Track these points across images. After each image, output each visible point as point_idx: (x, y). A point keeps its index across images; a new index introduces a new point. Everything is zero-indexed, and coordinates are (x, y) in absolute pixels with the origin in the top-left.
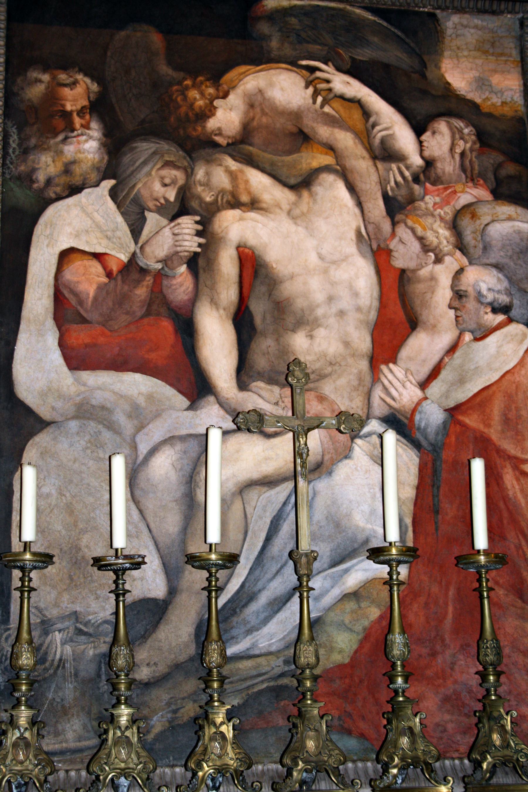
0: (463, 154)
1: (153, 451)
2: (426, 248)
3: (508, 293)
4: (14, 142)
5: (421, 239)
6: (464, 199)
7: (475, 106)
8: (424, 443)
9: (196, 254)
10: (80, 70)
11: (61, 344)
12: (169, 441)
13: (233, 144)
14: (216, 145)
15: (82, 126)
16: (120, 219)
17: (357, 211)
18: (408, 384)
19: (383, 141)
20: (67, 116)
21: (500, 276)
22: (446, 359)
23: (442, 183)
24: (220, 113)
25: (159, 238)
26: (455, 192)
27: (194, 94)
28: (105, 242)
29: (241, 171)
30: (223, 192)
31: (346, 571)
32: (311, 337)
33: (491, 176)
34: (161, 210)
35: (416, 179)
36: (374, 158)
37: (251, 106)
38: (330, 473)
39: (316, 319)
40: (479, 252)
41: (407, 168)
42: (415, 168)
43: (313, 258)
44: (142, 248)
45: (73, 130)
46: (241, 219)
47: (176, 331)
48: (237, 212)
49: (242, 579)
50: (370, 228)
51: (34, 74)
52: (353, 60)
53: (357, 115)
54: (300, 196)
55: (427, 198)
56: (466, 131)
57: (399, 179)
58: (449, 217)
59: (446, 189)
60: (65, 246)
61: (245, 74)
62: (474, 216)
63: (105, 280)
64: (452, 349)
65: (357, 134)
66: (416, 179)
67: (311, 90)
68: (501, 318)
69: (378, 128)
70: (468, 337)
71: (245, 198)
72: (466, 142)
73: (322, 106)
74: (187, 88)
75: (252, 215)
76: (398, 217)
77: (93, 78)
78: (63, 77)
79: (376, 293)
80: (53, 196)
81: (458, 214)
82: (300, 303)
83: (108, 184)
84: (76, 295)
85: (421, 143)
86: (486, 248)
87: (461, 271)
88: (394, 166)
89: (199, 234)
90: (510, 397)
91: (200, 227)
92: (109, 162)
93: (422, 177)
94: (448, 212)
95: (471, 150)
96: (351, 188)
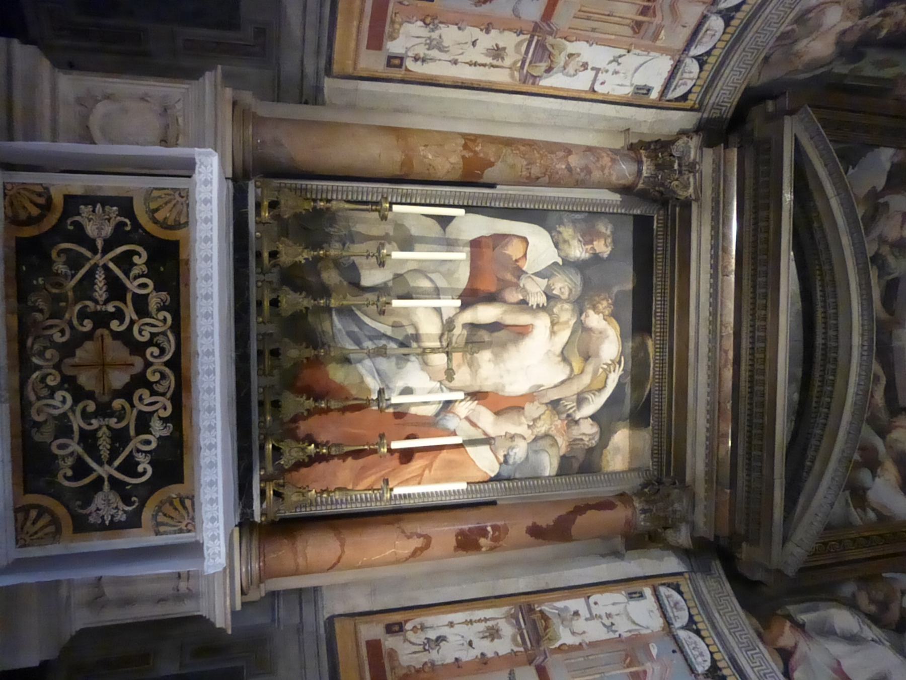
0: (582, 440)
1: (431, 280)
3: (514, 463)
4: (578, 216)
5: (539, 418)
7: (606, 446)
8: (438, 418)
9: (528, 304)
10: (613, 249)
13: (582, 324)
14: (581, 314)
15: (587, 249)
16: (543, 267)
17: (552, 385)
18: (467, 410)
19: (587, 399)
20: (591, 242)
21: (523, 459)
22: (480, 430)
23: (568, 429)
24: (596, 316)
26: (563, 436)
27: (605, 303)
30: (558, 317)
31: (374, 377)
32: (489, 361)
34: (548, 286)
35: (569, 416)
36: (578, 394)
37: (601, 333)
38: (422, 369)
41: (574, 411)
42: (574, 415)
44: (530, 277)
45: (585, 245)
46: (546, 327)
48: (549, 324)
49: (370, 324)
51: (610, 227)
52: (625, 384)
54: (558, 356)
55: (560, 421)
56: (594, 442)
57: (569, 407)
58: (550, 433)
59: (565, 431)
61: (615, 329)
62: (552, 445)
63: (514, 259)
65: (589, 385)
67: (610, 362)
68: (502, 459)
69: (593, 396)
71: (556, 328)
72: (588, 441)
73: (602, 368)
74: (608, 301)
75: (548, 332)
76: (550, 406)
77: (610, 255)
78: (609, 240)
80: (553, 234)
81: (552, 437)
82: (506, 355)
84: (506, 245)
85: (586, 418)
86: (536, 452)
87: (525, 439)
88: (575, 404)
89: (538, 305)
91: (541, 306)
92: (571, 262)
93: (570, 418)
94: (553, 432)
95: (584, 444)
96: (563, 382)
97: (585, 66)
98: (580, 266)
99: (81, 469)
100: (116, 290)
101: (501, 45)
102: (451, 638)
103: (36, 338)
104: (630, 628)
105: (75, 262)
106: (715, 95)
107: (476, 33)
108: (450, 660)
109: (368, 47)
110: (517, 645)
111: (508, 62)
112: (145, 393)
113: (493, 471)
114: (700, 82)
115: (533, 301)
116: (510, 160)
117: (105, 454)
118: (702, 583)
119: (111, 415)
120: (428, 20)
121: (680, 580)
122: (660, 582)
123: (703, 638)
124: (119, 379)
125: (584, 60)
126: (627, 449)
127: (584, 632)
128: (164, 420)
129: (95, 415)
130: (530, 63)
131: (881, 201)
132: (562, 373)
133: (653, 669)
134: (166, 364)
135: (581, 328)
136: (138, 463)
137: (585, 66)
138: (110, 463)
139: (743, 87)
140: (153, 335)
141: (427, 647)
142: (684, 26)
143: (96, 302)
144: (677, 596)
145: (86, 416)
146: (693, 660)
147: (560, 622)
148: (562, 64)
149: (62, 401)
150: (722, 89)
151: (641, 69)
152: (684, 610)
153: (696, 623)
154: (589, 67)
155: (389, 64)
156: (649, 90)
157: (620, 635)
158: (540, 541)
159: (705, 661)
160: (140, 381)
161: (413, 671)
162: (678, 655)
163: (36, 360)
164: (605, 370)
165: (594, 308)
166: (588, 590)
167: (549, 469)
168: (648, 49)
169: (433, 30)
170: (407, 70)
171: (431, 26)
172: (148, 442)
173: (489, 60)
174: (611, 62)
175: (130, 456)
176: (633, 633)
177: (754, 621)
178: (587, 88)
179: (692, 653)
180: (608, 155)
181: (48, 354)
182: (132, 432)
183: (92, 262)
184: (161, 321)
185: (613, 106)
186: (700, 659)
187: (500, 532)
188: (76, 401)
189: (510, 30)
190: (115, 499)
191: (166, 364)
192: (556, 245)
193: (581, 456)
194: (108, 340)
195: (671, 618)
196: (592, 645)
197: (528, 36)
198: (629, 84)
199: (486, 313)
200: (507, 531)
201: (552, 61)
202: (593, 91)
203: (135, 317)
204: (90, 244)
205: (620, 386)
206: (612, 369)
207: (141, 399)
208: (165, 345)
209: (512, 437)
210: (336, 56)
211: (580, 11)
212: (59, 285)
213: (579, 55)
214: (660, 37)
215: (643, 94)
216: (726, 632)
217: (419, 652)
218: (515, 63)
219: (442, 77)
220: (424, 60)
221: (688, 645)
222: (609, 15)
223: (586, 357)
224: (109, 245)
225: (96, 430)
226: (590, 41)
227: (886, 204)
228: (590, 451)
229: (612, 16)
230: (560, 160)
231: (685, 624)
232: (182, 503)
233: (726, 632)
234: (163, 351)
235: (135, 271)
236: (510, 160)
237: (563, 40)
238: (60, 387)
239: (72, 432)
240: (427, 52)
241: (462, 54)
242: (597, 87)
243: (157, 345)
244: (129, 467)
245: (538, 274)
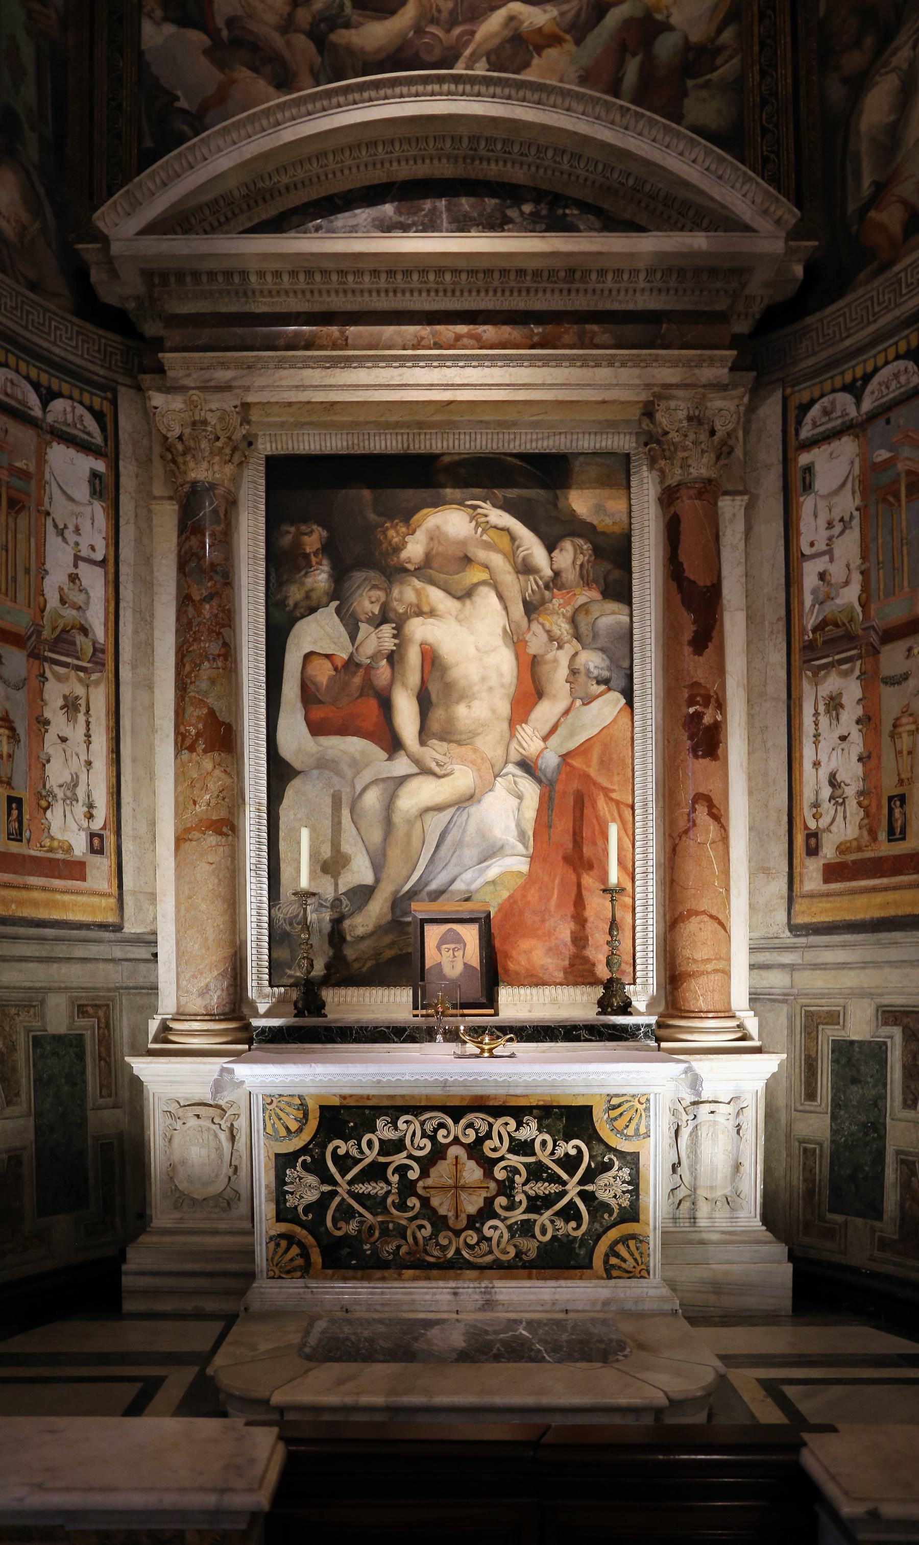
0: (582, 566)
1: (365, 789)
2: (551, 638)
5: (548, 632)
6: (581, 600)
7: (592, 527)
8: (544, 779)
9: (393, 651)
11: (307, 719)
12: (375, 782)
14: (406, 570)
16: (342, 629)
17: (504, 613)
19: (524, 559)
20: (306, 556)
24: (410, 547)
25: (368, 641)
27: (391, 533)
28: (333, 646)
29: (424, 589)
30: (411, 605)
31: (488, 867)
33: (602, 582)
34: (369, 621)
35: (547, 587)
36: (518, 572)
37: (432, 539)
38: (479, 801)
39: (473, 694)
40: (590, 639)
41: (541, 578)
42: (546, 579)
43: (472, 651)
47: (380, 707)
50: (513, 626)
51: (285, 528)
53: (506, 540)
54: (464, 605)
56: (585, 547)
57: (535, 587)
58: (569, 614)
60: (307, 650)
61: (427, 515)
62: (587, 612)
64: (567, 712)
65: (505, 555)
66: (547, 587)
67: (474, 523)
68: (603, 687)
70: (578, 703)
71: (426, 609)
74: (387, 529)
75: (431, 620)
76: (533, 616)
77: (324, 527)
78: (303, 528)
79: (515, 674)
81: (576, 611)
82: (462, 683)
83: (335, 604)
84: (314, 684)
85: (551, 558)
86: (595, 636)
87: (576, 654)
88: (531, 578)
89: (395, 637)
90: (605, 746)
92: (335, 589)
95: (588, 562)
96: (500, 597)
97: (74, 578)
98: (340, 576)
99: (570, 1213)
100: (376, 1172)
101: (60, 702)
102: (833, 765)
103: (426, 1252)
104: (850, 494)
105: (346, 1213)
106: (90, 366)
107: (51, 737)
108: (859, 769)
109: (84, 880)
110: (852, 670)
111: (80, 691)
112: (488, 1144)
113: (619, 700)
114: (76, 394)
115: (389, 644)
116: (204, 685)
117: (554, 1188)
118: (803, 365)
119: (512, 1181)
120: (44, 803)
121: (794, 402)
122: (793, 437)
123: (876, 370)
124: (472, 1172)
125: (66, 579)
126: (598, 491)
127: (848, 566)
128: (519, 1124)
129: (510, 1197)
130: (78, 658)
131: (225, 33)
132: (488, 600)
133: (907, 459)
134: (456, 1122)
136: (567, 1154)
137: (74, 578)
138: (564, 1183)
139: (76, 320)
140: (424, 1135)
141: (840, 800)
142: (6, 431)
143: (388, 1193)
144: (816, 410)
145: (511, 1207)
146: (902, 390)
147: (831, 603)
148: (74, 612)
149: (494, 1229)
150: (82, 357)
151: (69, 491)
152: (834, 399)
153: (855, 380)
154: (75, 571)
155: (100, 851)
156: (95, 475)
157: (857, 509)
158: (715, 634)
159: (906, 369)
160: (475, 1150)
161: (866, 821)
162: (893, 415)
163: (450, 1254)
164: (484, 531)
165: (398, 549)
166: (795, 555)
167: (621, 617)
168: (42, 484)
169: (55, 797)
170: (104, 828)
171: (50, 799)
172: (544, 1143)
173: (81, 717)
174: (65, 540)
175: (558, 1162)
176: (857, 488)
177: (862, 276)
178: (99, 571)
179: (894, 391)
180: (187, 538)
181: (444, 1242)
182: (531, 1159)
183: (346, 1196)
184: (408, 1126)
185: (121, 530)
186: (903, 379)
187: (697, 695)
188: (495, 1216)
189: (41, 691)
190: (605, 1178)
191: (456, 1122)
192: (312, 610)
193: (605, 566)
194: (429, 1182)
195: (843, 423)
196: (864, 557)
197: (46, 665)
198: (89, 509)
200: (696, 684)
201: (73, 627)
202: (103, 563)
203: (404, 1154)
204: (327, 1198)
205: (507, 507)
206: (483, 519)
207: (495, 1150)
208: (435, 1123)
209: (574, 672)
210: (99, 919)
211: (6, 594)
212: (371, 1228)
213: (61, 589)
214: (25, 467)
215: (101, 483)
216: (872, 328)
217: (845, 812)
218: (80, 680)
219: (108, 780)
220: (91, 806)
221: (883, 397)
222: (7, 551)
223: (467, 560)
224: (326, 1178)
225: (528, 1197)
226: (43, 573)
227: (231, 22)
228: (598, 552)
229: (7, 546)
230: (199, 613)
231: (854, 400)
232: (614, 1108)
233: (872, 328)
234: (442, 1125)
235: (354, 1152)
236: (204, 685)
237: (46, 614)
238: (479, 1231)
239: (528, 1220)
240: (80, 803)
241: (77, 755)
242: (99, 556)
243: (435, 1131)
244: (570, 1163)
245: (353, 637)
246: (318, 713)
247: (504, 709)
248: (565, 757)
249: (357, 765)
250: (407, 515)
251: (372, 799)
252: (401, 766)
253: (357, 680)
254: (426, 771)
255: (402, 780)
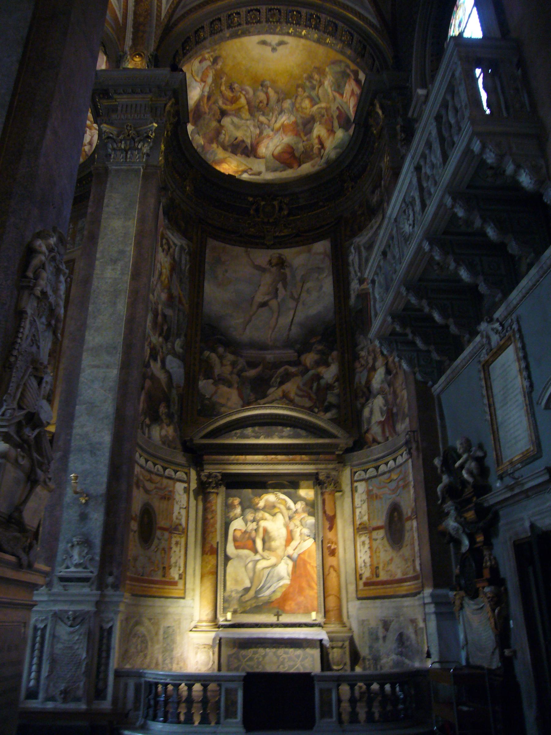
2: (295, 525)
20: (235, 506)
27: (256, 500)
51: (230, 498)
53: (284, 502)
60: (234, 528)
64: (299, 543)
68: (308, 537)
70: (302, 541)
86: (306, 525)
94: (300, 518)
96: (283, 515)
98: (243, 510)
115: (255, 527)
135: (264, 509)
165: (258, 504)
170: (182, 573)
192: (236, 518)
193: (308, 508)
199: (259, 544)
205: (284, 493)
209: (301, 534)
228: (307, 504)
245: (246, 524)
246: (237, 544)
247: (284, 543)
248: (299, 555)
249: (247, 557)
250: (260, 496)
251: (250, 565)
252: (258, 557)
253: (247, 536)
254: (264, 558)
255: (258, 561)
